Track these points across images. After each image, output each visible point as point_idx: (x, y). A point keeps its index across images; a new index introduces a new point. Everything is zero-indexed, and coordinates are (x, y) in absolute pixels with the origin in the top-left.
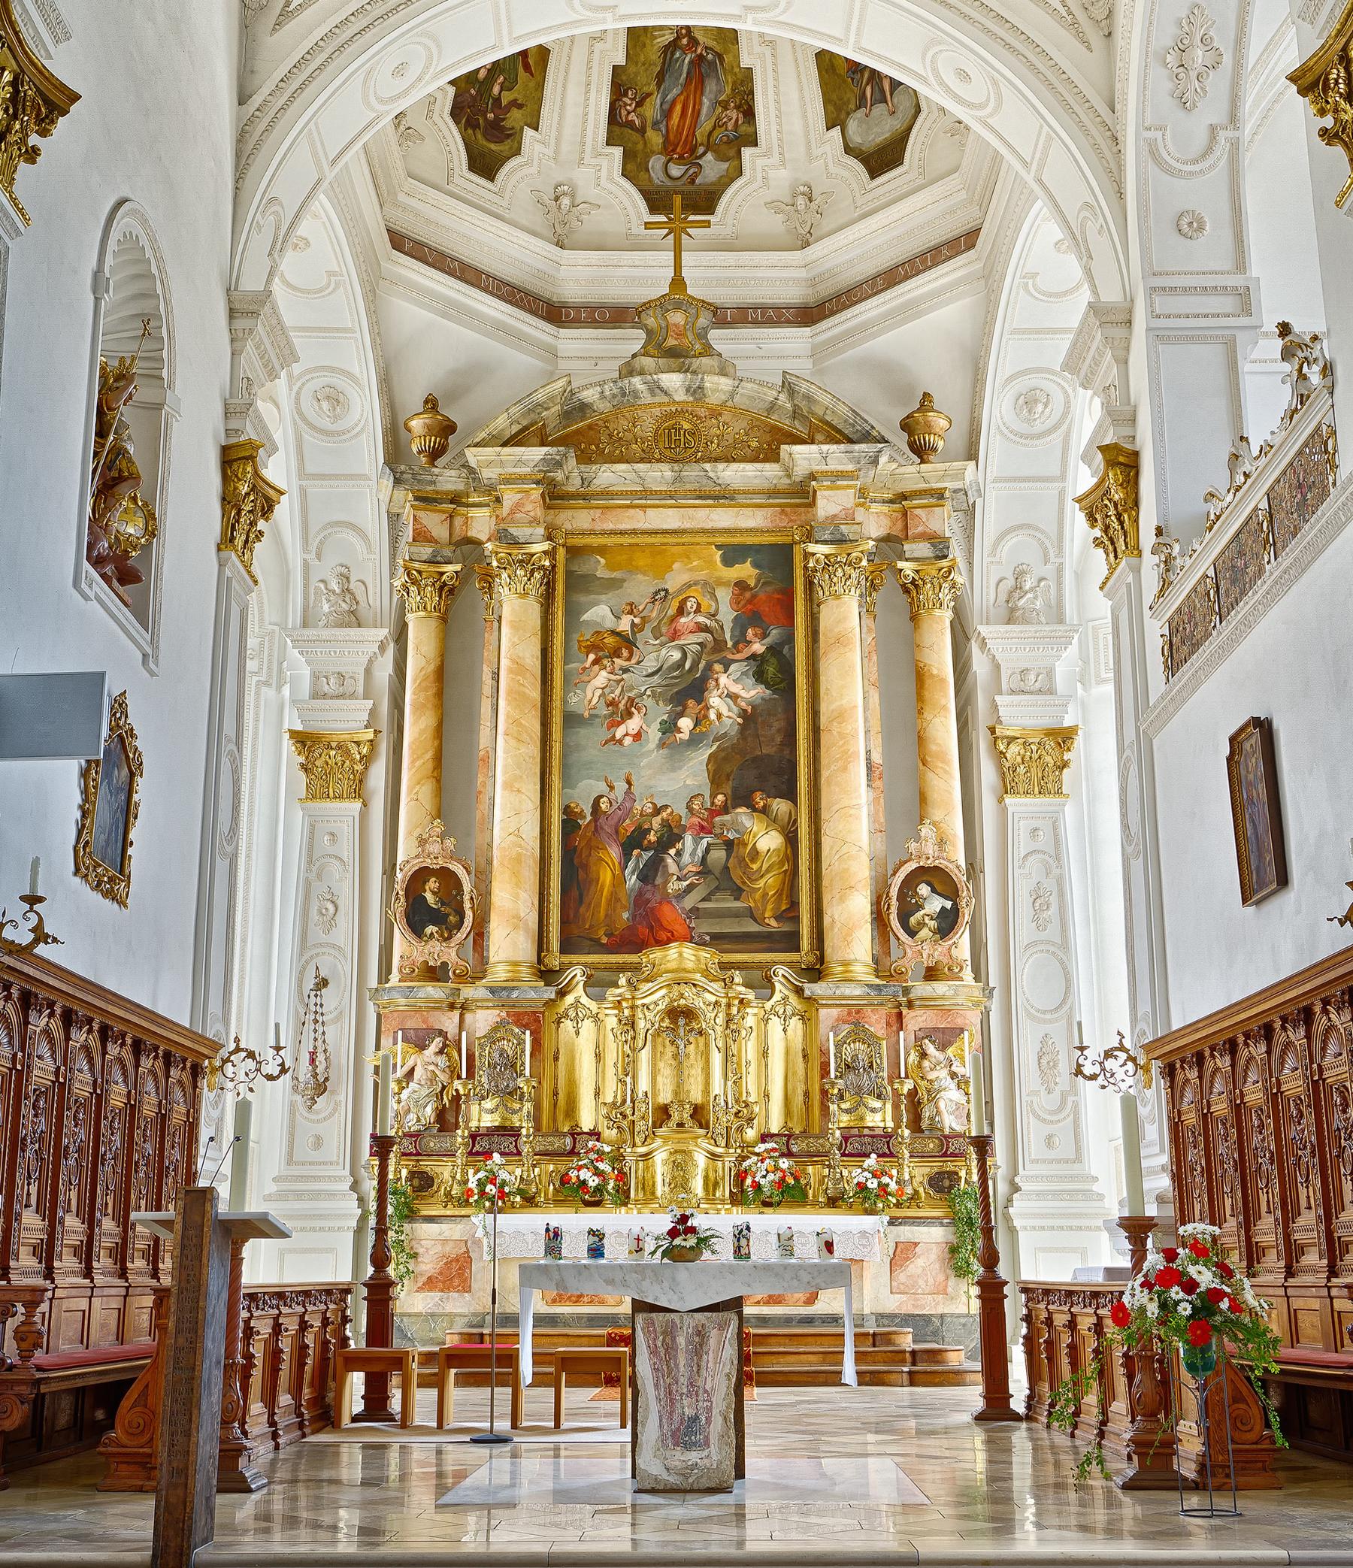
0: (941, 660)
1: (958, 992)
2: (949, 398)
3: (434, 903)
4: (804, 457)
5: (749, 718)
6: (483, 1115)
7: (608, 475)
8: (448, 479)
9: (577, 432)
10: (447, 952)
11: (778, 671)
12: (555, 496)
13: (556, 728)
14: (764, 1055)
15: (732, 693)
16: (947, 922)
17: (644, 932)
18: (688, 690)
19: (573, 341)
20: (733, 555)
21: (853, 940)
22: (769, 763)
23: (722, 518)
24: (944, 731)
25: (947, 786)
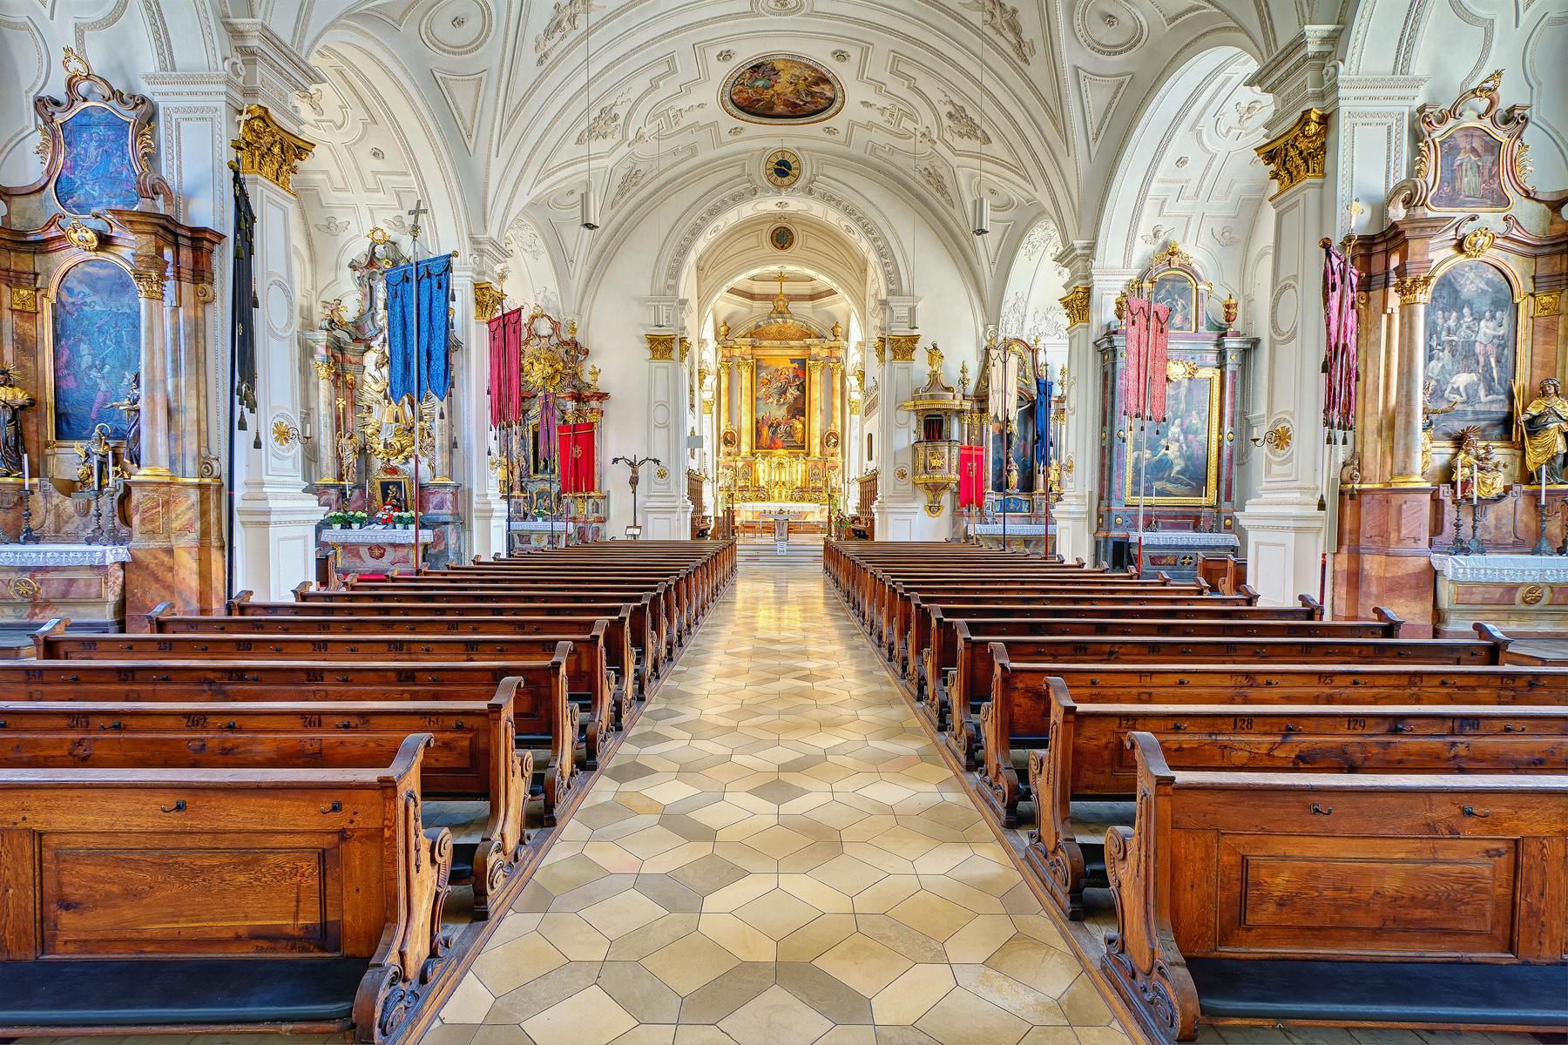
0: (838, 386)
1: (838, 460)
2: (842, 323)
3: (729, 440)
4: (809, 341)
5: (796, 399)
6: (741, 483)
7: (765, 343)
8: (730, 343)
9: (757, 334)
10: (733, 450)
11: (802, 388)
12: (753, 347)
13: (755, 401)
14: (797, 471)
15: (792, 393)
16: (836, 444)
17: (772, 446)
18: (783, 392)
19: (756, 304)
20: (793, 361)
21: (816, 449)
22: (799, 409)
23: (791, 352)
24: (838, 402)
25: (838, 415)
